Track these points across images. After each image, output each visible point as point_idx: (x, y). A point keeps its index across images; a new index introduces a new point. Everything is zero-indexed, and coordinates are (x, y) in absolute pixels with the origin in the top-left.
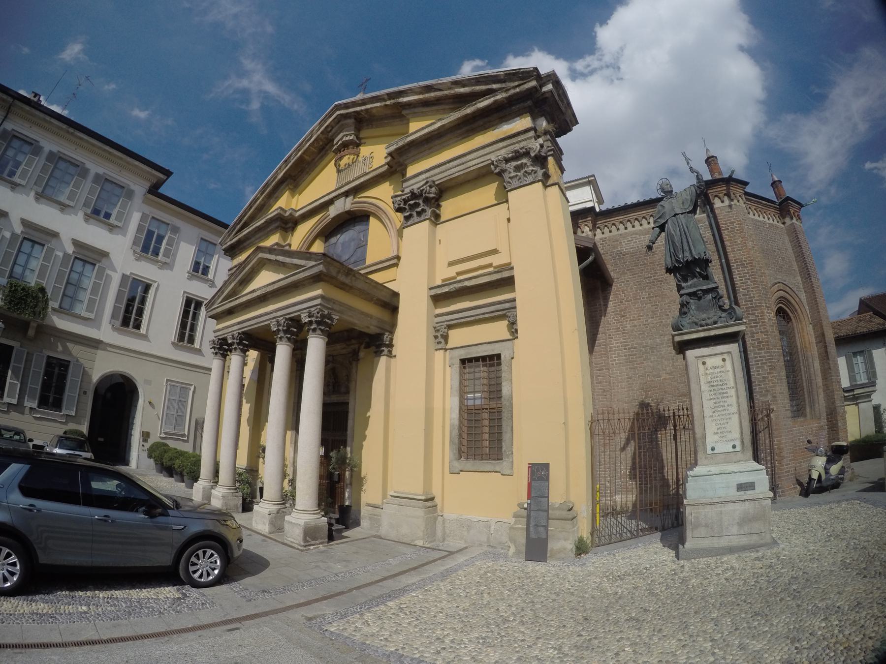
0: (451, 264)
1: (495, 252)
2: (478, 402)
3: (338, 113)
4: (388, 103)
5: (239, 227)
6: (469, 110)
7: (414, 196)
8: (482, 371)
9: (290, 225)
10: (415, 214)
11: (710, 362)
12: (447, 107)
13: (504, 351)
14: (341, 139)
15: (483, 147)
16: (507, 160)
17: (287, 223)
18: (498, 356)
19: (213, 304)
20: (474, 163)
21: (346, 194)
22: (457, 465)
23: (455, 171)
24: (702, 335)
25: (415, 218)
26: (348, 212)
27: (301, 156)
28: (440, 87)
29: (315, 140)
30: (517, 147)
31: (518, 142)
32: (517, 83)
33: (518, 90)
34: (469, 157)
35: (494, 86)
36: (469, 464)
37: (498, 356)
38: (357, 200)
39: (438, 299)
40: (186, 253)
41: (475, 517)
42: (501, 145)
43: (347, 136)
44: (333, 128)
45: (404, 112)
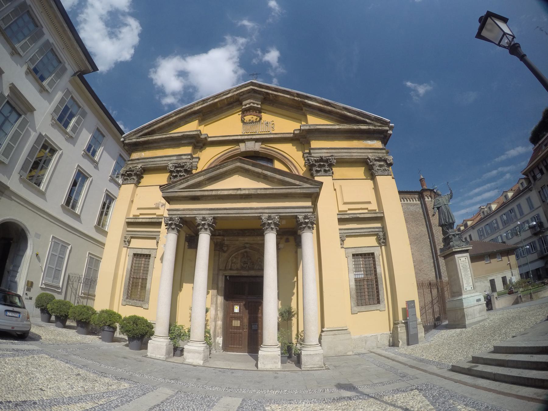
0: (345, 203)
1: (370, 203)
2: (362, 276)
3: (251, 87)
4: (296, 98)
5: (147, 131)
6: (355, 127)
7: (321, 159)
8: (361, 260)
9: (201, 145)
10: (322, 170)
11: (461, 259)
12: (335, 118)
13: (377, 252)
14: (249, 104)
16: (376, 160)
17: (199, 142)
18: (373, 254)
19: (171, 188)
20: (356, 155)
21: (257, 140)
22: (356, 309)
23: (345, 155)
24: (461, 249)
25: (322, 173)
26: (255, 152)
27: (216, 103)
28: (336, 107)
29: (231, 97)
30: (381, 155)
31: (378, 153)
32: (379, 124)
33: (380, 128)
34: (352, 151)
35: (367, 120)
36: (363, 308)
37: (373, 254)
38: (263, 146)
40: (85, 137)
41: (368, 334)
42: (369, 151)
43: (254, 103)
44: (244, 94)
45: (304, 108)
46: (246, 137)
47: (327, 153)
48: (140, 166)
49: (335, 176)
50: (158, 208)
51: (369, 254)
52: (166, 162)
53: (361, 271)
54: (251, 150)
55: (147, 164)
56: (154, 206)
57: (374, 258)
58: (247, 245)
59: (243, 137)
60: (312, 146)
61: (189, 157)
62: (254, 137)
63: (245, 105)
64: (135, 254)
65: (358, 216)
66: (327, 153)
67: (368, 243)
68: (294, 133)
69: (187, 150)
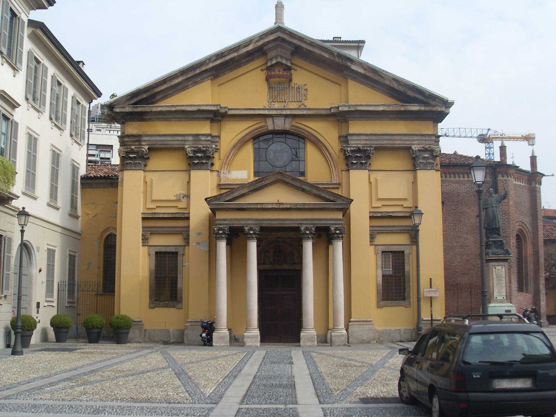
7: (358, 150)
15: (405, 135)
17: (217, 116)
18: (403, 252)
20: (398, 143)
23: (386, 143)
25: (359, 165)
37: (403, 252)
39: (371, 218)
43: (282, 57)
46: (274, 112)
47: (366, 140)
48: (146, 147)
49: (372, 168)
50: (179, 200)
51: (399, 252)
52: (179, 142)
53: (389, 268)
54: (280, 129)
55: (154, 143)
56: (175, 198)
57: (404, 256)
58: (280, 240)
59: (271, 112)
60: (351, 131)
61: (209, 138)
62: (284, 112)
63: (271, 60)
64: (156, 253)
65: (391, 214)
66: (366, 140)
67: (398, 240)
68: (330, 109)
69: (204, 128)
